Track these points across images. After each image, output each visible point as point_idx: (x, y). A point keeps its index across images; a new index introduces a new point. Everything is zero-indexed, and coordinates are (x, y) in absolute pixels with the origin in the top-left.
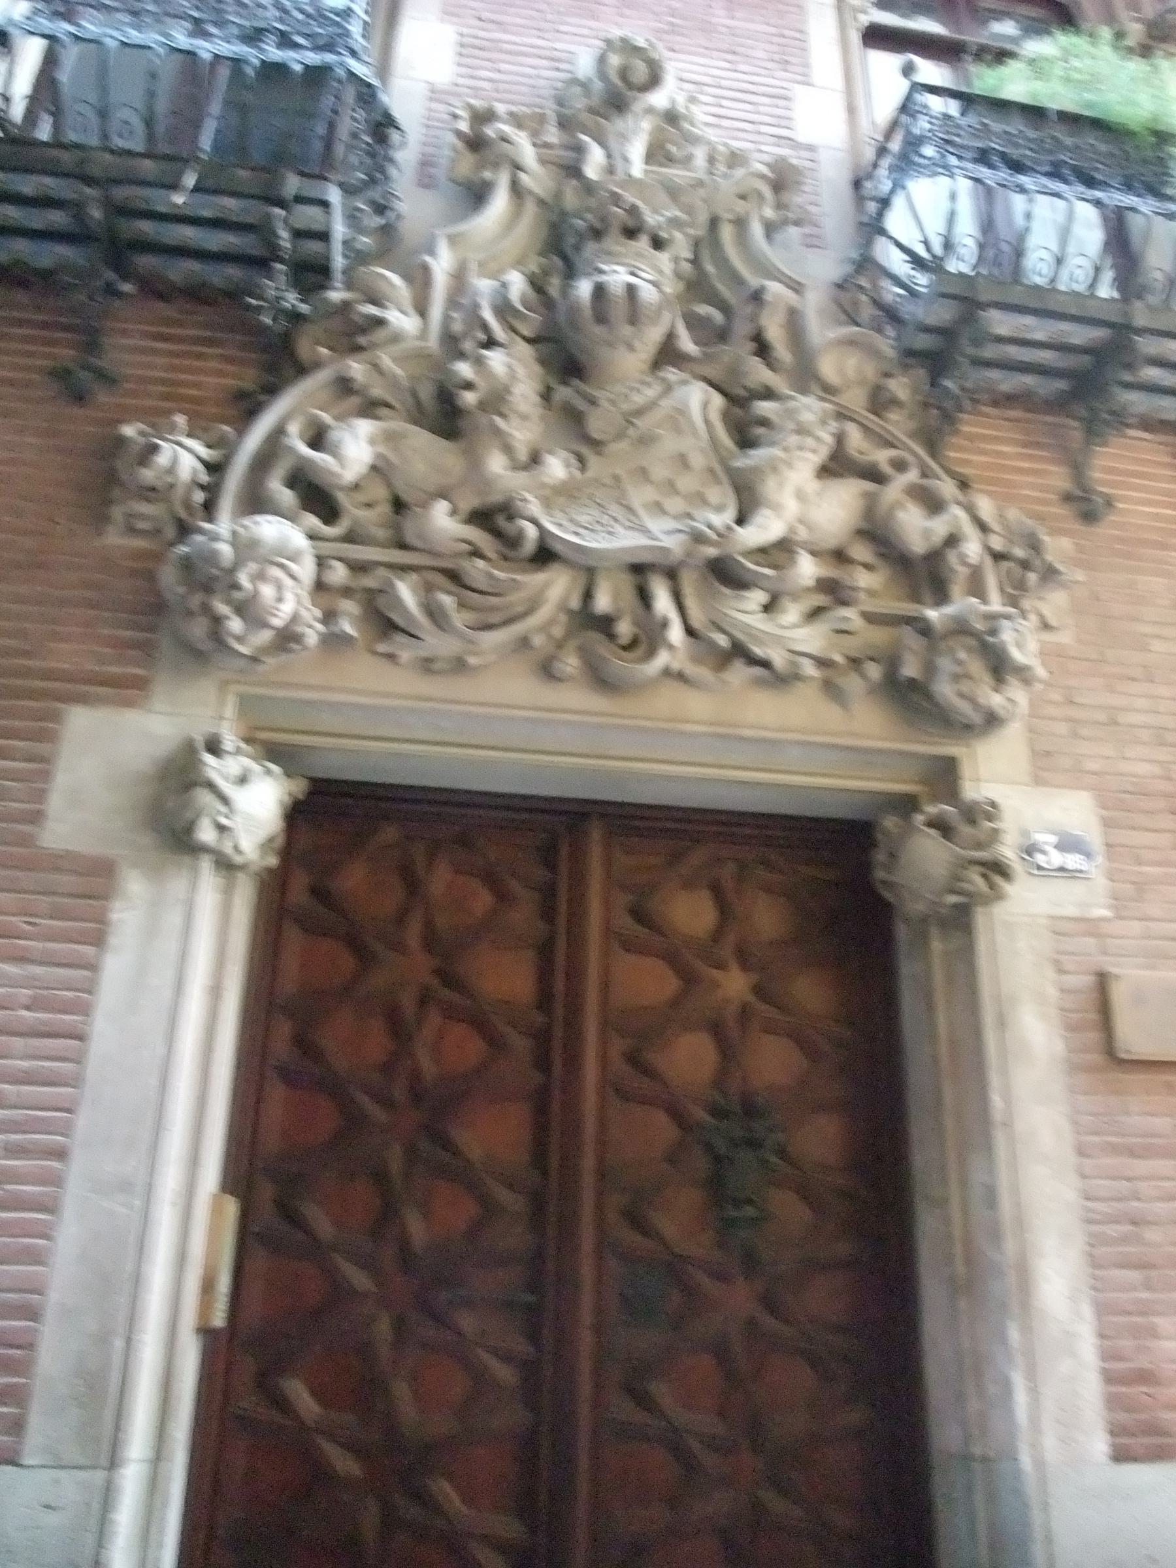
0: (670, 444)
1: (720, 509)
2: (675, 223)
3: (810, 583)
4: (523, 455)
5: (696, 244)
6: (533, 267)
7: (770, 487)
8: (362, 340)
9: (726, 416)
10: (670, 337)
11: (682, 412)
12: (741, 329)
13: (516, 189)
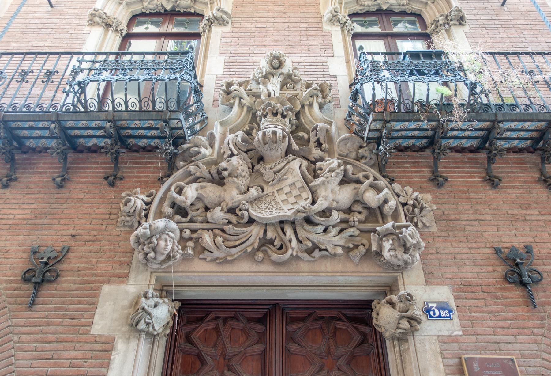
0: (290, 180)
1: (306, 199)
2: (290, 110)
3: (339, 220)
4: (244, 188)
5: (298, 115)
6: (247, 128)
7: (321, 193)
8: (193, 159)
10: (290, 144)
12: (313, 139)
13: (241, 106)
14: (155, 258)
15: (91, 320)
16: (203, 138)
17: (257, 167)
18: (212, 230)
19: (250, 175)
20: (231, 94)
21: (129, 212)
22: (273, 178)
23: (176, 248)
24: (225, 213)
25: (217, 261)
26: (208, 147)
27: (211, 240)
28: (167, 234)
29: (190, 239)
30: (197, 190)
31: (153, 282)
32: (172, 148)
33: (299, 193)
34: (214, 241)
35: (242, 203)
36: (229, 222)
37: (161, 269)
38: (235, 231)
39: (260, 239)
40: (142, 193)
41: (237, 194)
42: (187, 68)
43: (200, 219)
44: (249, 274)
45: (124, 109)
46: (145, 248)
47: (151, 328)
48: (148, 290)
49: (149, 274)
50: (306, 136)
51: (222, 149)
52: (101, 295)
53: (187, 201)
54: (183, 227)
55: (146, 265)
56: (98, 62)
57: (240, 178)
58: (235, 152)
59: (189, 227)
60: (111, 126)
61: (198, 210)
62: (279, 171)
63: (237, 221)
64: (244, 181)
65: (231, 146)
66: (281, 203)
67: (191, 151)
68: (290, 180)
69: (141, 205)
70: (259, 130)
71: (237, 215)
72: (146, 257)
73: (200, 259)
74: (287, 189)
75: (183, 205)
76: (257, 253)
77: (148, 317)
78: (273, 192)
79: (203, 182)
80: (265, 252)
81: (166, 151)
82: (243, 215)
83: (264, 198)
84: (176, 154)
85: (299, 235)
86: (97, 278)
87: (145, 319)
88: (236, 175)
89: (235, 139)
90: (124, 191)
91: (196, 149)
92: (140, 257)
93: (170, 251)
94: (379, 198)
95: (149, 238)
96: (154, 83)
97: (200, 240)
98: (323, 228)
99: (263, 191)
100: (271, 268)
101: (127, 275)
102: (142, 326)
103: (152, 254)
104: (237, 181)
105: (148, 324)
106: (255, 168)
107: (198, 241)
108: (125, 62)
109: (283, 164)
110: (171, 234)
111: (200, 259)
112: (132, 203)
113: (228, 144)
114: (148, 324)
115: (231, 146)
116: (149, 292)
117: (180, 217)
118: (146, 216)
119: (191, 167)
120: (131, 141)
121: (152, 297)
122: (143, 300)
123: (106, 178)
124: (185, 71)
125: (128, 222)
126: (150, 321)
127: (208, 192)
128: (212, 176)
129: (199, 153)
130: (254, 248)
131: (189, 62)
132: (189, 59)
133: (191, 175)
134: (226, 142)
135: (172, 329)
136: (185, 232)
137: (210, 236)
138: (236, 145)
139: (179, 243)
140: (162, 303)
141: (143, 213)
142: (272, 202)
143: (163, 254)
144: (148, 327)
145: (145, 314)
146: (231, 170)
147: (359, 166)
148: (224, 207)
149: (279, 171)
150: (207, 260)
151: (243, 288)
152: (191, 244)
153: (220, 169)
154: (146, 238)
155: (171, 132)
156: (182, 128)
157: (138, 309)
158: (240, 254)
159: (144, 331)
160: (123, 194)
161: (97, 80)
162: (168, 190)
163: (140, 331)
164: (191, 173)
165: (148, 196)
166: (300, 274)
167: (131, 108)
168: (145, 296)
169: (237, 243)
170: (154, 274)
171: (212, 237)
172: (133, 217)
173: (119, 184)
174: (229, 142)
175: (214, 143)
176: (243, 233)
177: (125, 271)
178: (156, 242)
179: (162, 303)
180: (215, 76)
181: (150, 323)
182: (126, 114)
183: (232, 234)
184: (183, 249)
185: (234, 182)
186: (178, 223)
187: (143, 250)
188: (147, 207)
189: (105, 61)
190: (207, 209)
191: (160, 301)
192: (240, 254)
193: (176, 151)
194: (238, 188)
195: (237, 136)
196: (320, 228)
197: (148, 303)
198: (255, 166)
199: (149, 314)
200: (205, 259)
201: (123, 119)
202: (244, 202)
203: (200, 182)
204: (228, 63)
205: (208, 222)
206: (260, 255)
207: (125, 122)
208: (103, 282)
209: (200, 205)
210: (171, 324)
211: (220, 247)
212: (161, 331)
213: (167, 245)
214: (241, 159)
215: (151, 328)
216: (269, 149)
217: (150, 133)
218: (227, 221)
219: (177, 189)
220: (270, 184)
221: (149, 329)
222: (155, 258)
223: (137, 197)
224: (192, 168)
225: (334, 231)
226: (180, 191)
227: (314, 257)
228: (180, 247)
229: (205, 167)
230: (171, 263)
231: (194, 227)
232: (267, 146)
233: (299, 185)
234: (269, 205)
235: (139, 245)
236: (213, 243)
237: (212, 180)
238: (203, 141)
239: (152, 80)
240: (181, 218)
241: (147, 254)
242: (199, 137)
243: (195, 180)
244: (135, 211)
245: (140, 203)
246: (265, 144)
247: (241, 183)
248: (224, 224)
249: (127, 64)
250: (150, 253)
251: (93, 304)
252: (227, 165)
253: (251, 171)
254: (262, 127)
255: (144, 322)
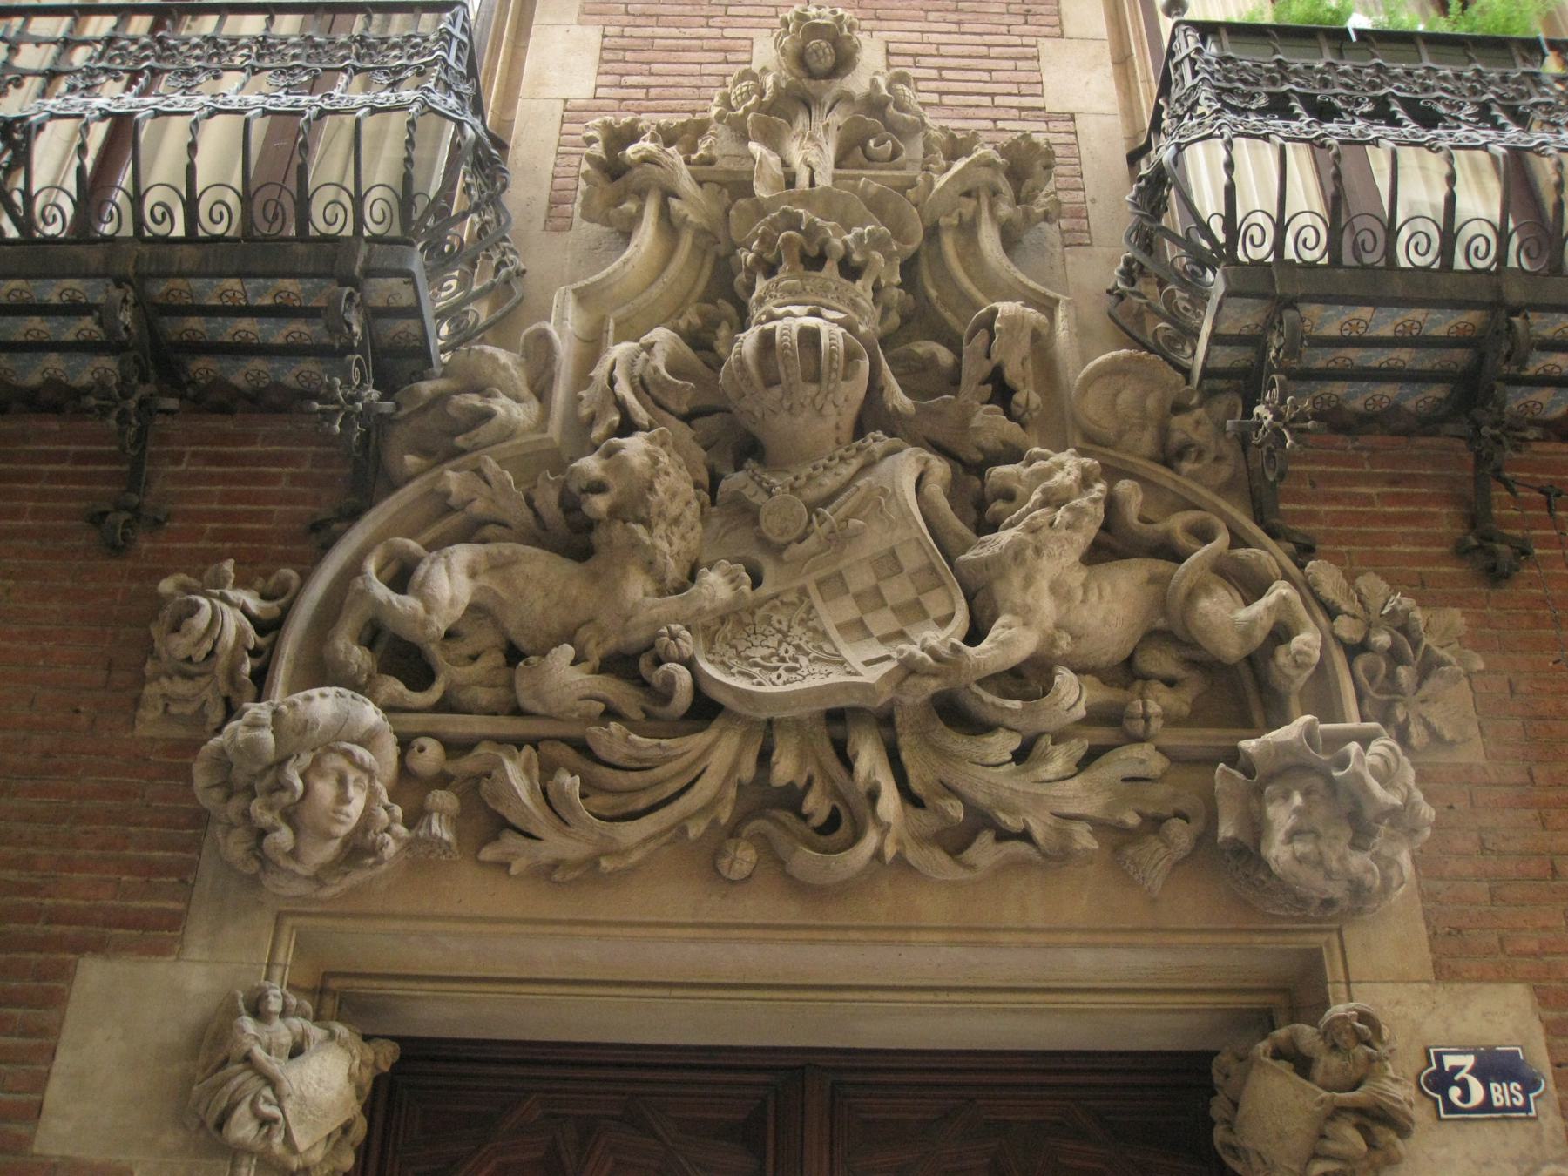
0: (875, 540)
1: (944, 622)
2: (878, 242)
3: (1080, 711)
4: (674, 571)
6: (691, 317)
7: (1011, 589)
8: (460, 441)
9: (954, 491)
10: (875, 388)
11: (888, 493)
12: (974, 369)
13: (669, 225)
14: (294, 854)
15: (37, 1097)
16: (503, 356)
17: (734, 481)
18: (535, 743)
19: (704, 518)
20: (628, 176)
21: (189, 659)
22: (801, 529)
23: (383, 814)
24: (593, 672)
25: (557, 877)
26: (524, 391)
27: (532, 787)
28: (348, 754)
29: (443, 780)
30: (473, 574)
31: (285, 954)
32: (375, 394)
33: (910, 594)
34: (545, 792)
35: (665, 630)
36: (611, 713)
37: (322, 902)
38: (633, 752)
39: (740, 786)
40: (242, 583)
41: (646, 594)
42: (447, 68)
43: (484, 696)
44: (690, 933)
45: (179, 231)
46: (256, 807)
47: (277, 1140)
48: (267, 984)
49: (270, 919)
50: (944, 356)
51: (584, 403)
52: (73, 996)
53: (435, 618)
54: (413, 729)
55: (254, 882)
56: (86, 42)
57: (661, 528)
58: (641, 414)
59: (439, 728)
60: (125, 301)
61: (474, 658)
62: (828, 500)
63: (644, 711)
64: (676, 539)
65: (623, 389)
66: (834, 634)
67: (450, 410)
68: (875, 540)
69: (241, 633)
70: (744, 328)
71: (644, 684)
72: (259, 846)
73: (483, 864)
74: (862, 579)
75: (411, 633)
76: (730, 845)
77: (267, 1092)
78: (803, 592)
79: (499, 539)
80: (764, 844)
81: (350, 407)
82: (670, 681)
83: (760, 613)
84: (385, 420)
85: (912, 774)
86: (58, 929)
87: (253, 1103)
88: (642, 513)
89: (639, 362)
90: (165, 574)
91: (474, 400)
92: (236, 847)
93: (356, 829)
94: (1253, 622)
95: (270, 767)
96: (308, 121)
97: (485, 785)
98: (1016, 743)
99: (756, 582)
100: (791, 911)
101: (175, 922)
102: (243, 1129)
103: (284, 837)
104: (647, 539)
105: (266, 1122)
106: (723, 486)
107: (477, 787)
108: (195, 40)
109: (846, 471)
110: (359, 751)
111: (483, 864)
112: (202, 620)
113: (612, 381)
114: (266, 1122)
115: (623, 389)
116: (271, 992)
117: (401, 687)
118: (261, 678)
119: (450, 474)
120: (202, 367)
121: (284, 1014)
122: (249, 1024)
123: (97, 519)
124: (438, 79)
125: (185, 700)
126: (275, 1111)
127: (520, 582)
128: (537, 514)
129: (488, 415)
130: (715, 822)
131: (455, 44)
132: (456, 31)
133: (449, 510)
134: (600, 372)
135: (363, 1152)
136: (422, 750)
137: (527, 771)
138: (642, 386)
139: (393, 796)
140: (321, 1043)
141: (247, 667)
142: (797, 630)
143: (329, 836)
144: (268, 1136)
145: (255, 1083)
146: (620, 493)
147: (1171, 486)
148: (591, 646)
149: (828, 500)
150: (514, 871)
151: (665, 992)
152: (443, 799)
153: (574, 487)
154: (258, 768)
155: (367, 326)
156: (415, 312)
157: (225, 1062)
158: (651, 846)
159: (252, 1154)
160: (166, 586)
161: (76, 111)
162: (354, 568)
163: (235, 1153)
164: (452, 501)
165: (264, 597)
166: (913, 936)
167: (207, 228)
168: (258, 1010)
169: (643, 802)
170: (289, 922)
171: (536, 772)
172: (202, 681)
173: (146, 545)
174: (617, 373)
175: (552, 379)
176: (667, 760)
177: (171, 905)
178: (299, 784)
179: (321, 1043)
180: (559, 106)
181: (276, 1120)
182: (187, 250)
183: (621, 763)
184: (409, 822)
185: (636, 544)
186: (389, 709)
187: (246, 815)
188: (262, 641)
189: (110, 41)
190: (513, 655)
191: (317, 1033)
192: (651, 846)
193: (388, 406)
194: (650, 566)
195: (649, 348)
196: (1002, 745)
197: (265, 1038)
198: (722, 477)
199: (271, 1082)
200: (507, 866)
201: (175, 269)
202: (675, 627)
203: (484, 541)
204: (611, 55)
205: (517, 711)
206: (744, 858)
207: (179, 283)
208: (82, 947)
209: (484, 638)
210: (360, 1130)
211: (567, 818)
212: (317, 1155)
213: (343, 799)
214: (663, 445)
215: (277, 1140)
216: (786, 404)
217: (280, 332)
218: (601, 706)
219: (392, 568)
220: (786, 555)
221: (270, 1147)
222: (294, 854)
223: (224, 598)
224: (453, 479)
225: (1058, 761)
226: (402, 577)
227: (972, 867)
228: (398, 811)
229: (510, 477)
230: (356, 878)
231: (460, 730)
232: (776, 392)
233: (911, 559)
234: (780, 643)
235: (229, 797)
236: (541, 799)
237: (540, 536)
238: (504, 367)
239: (302, 114)
240: (407, 692)
241: (262, 833)
242: (489, 349)
243: (471, 532)
244: (211, 654)
245: (232, 621)
246: (771, 381)
247: (664, 545)
248: (587, 720)
249: (198, 52)
250: (276, 829)
251: (42, 1032)
252: (605, 469)
253: (706, 497)
254: (757, 313)
255: (248, 1114)
